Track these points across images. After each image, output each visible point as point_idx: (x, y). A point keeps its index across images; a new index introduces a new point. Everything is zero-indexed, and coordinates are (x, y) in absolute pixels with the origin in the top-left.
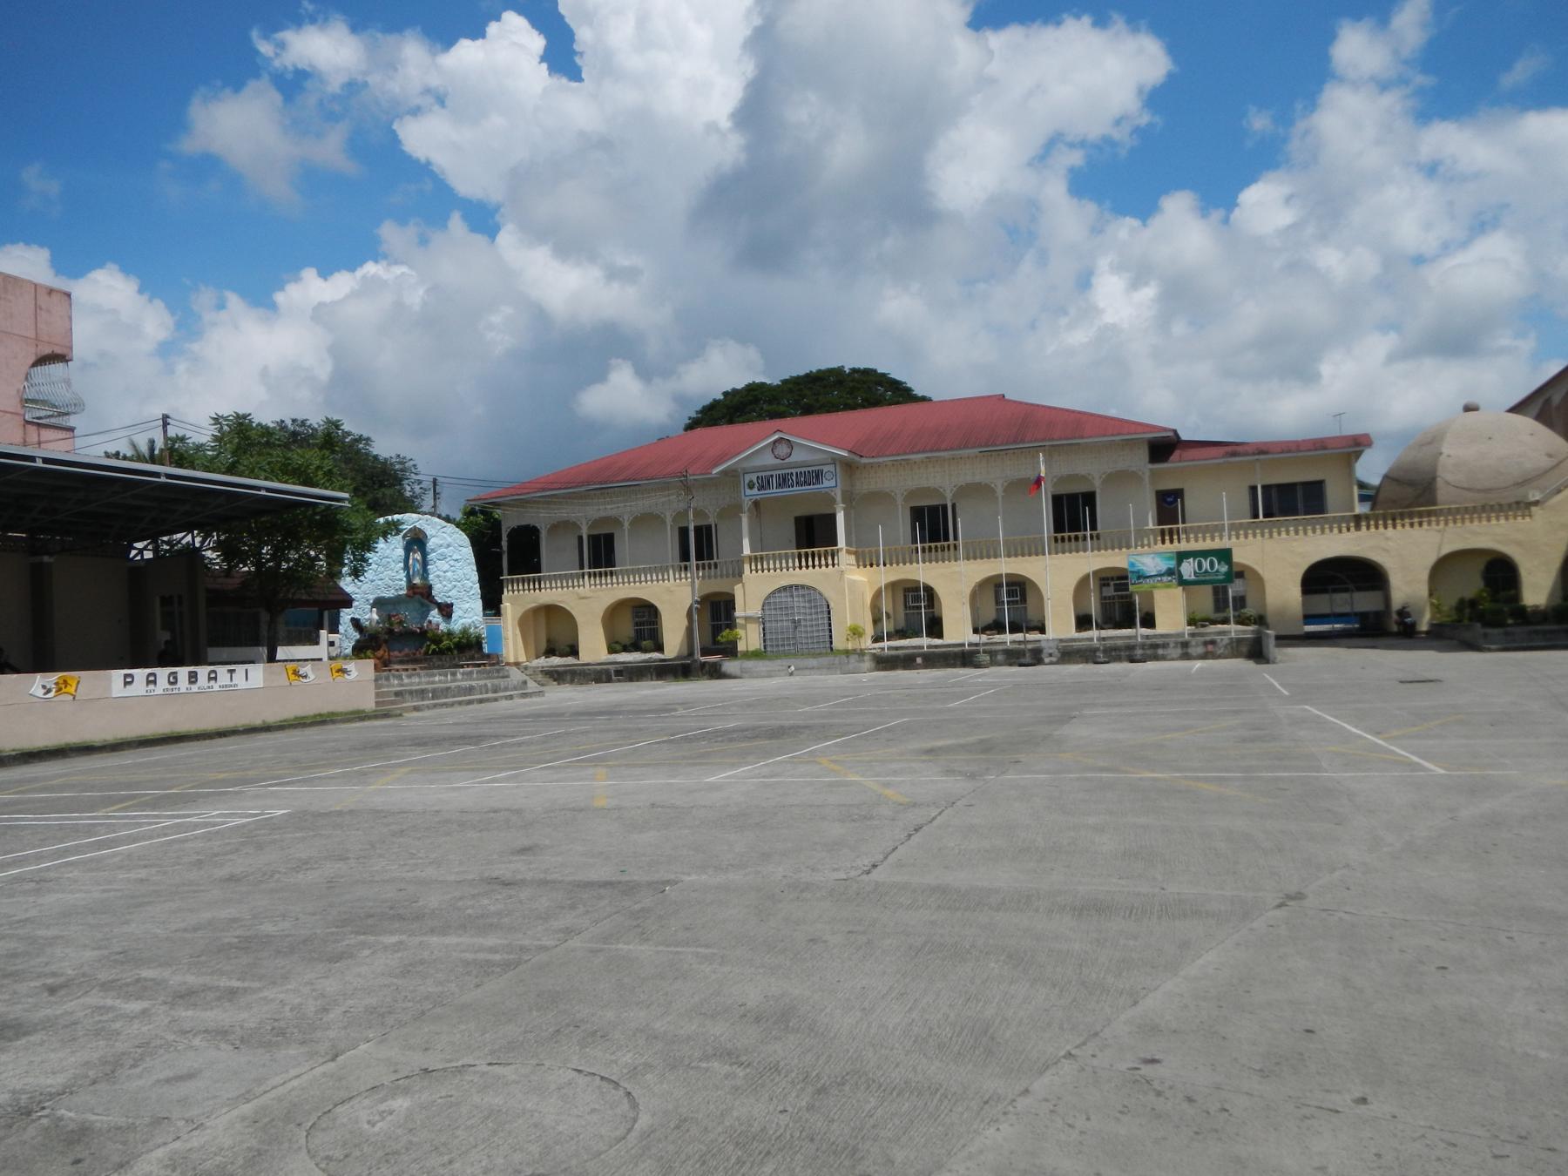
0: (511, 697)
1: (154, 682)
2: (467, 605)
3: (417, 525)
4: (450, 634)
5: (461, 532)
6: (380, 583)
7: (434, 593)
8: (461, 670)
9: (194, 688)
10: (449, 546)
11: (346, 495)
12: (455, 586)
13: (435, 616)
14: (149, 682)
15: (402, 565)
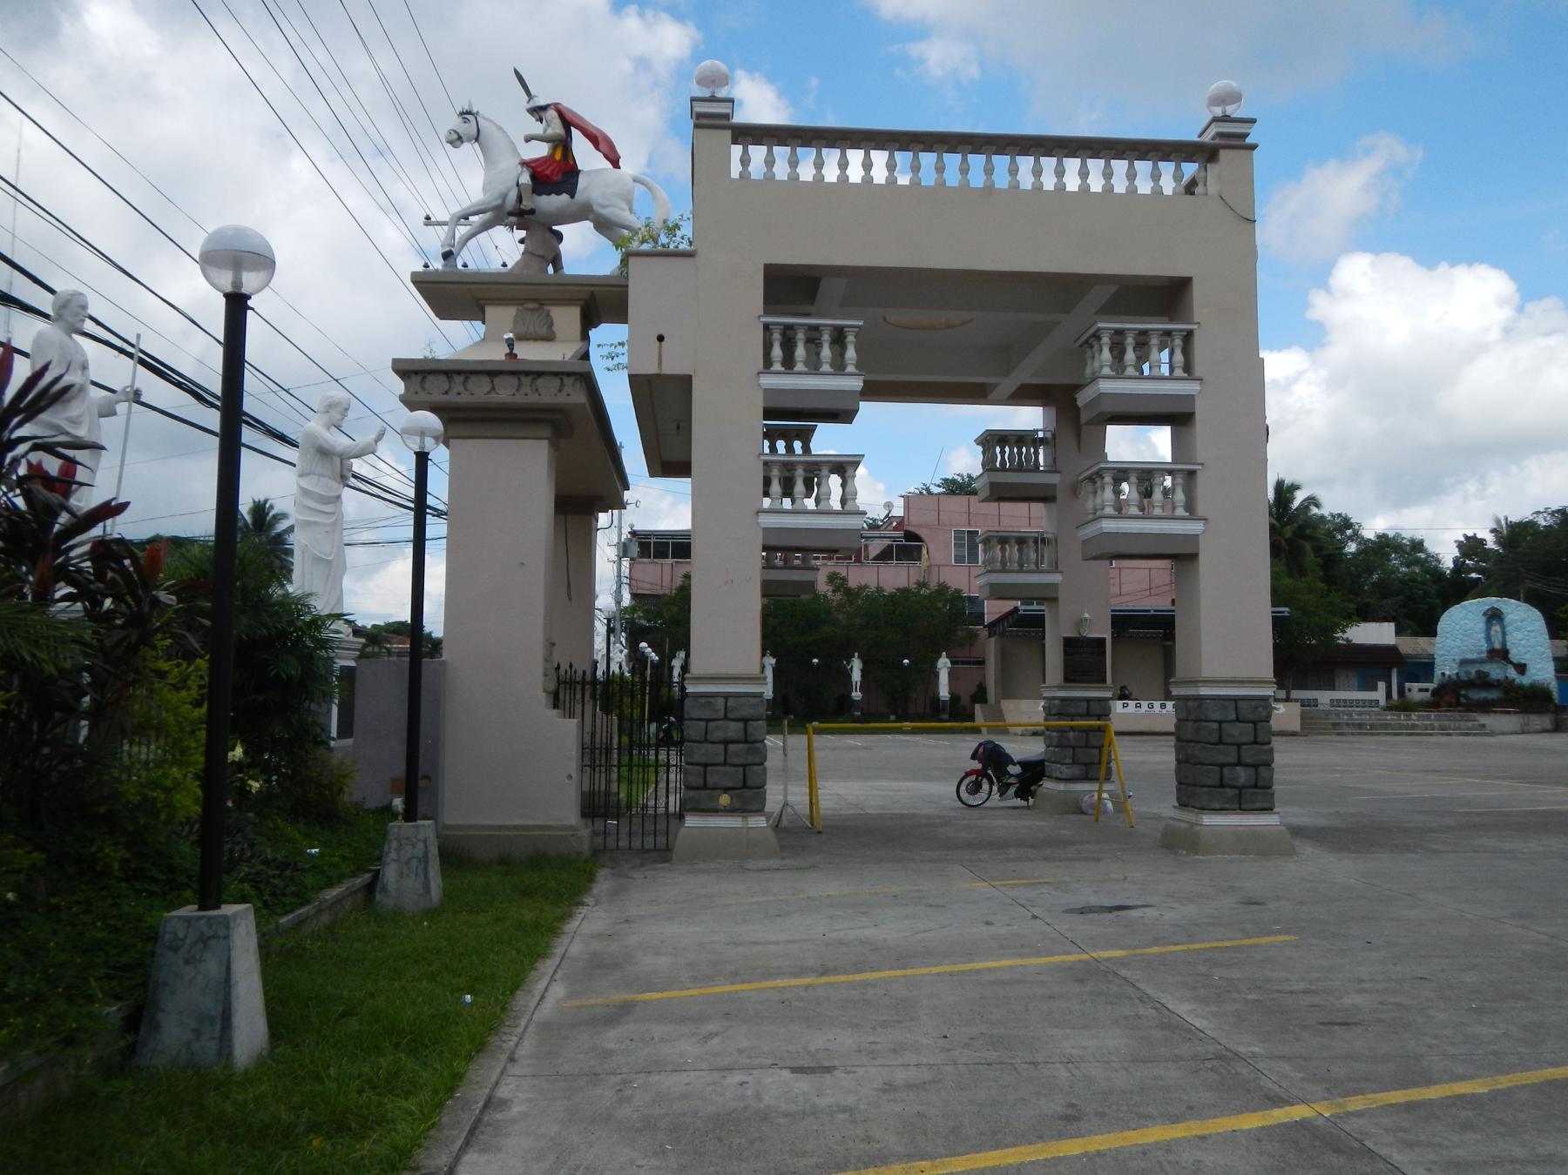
0: (1449, 735)
1: (1140, 707)
2: (1539, 666)
3: (1495, 606)
4: (1521, 687)
5: (1534, 610)
6: (1465, 648)
7: (1510, 656)
8: (1417, 713)
9: (1164, 711)
10: (1523, 620)
11: (1287, 609)
12: (1529, 651)
13: (1512, 673)
14: (1136, 707)
15: (1483, 635)
